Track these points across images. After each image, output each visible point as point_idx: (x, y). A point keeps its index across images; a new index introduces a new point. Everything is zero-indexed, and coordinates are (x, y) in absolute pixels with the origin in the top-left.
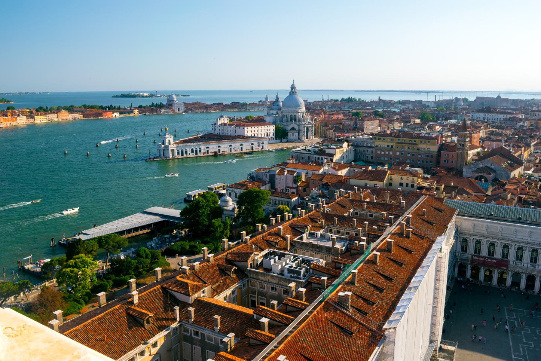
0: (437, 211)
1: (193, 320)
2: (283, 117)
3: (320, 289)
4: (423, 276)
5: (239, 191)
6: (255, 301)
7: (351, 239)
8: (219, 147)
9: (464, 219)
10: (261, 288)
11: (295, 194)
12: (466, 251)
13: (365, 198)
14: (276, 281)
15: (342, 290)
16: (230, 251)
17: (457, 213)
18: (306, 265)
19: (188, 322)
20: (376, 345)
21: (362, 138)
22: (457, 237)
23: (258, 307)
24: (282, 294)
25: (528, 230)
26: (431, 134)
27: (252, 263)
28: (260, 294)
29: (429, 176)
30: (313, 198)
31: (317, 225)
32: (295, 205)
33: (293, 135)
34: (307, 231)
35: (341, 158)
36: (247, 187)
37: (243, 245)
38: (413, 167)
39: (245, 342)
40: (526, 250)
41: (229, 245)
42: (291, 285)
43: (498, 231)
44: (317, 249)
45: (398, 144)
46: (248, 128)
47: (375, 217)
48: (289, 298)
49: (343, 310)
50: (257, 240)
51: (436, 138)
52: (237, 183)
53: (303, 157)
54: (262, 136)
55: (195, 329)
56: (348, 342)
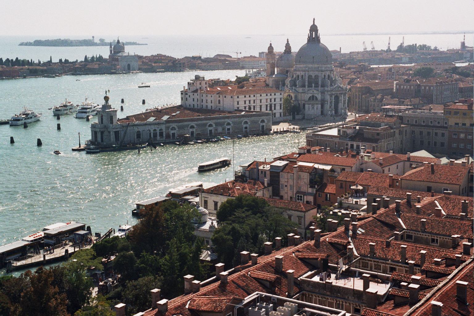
2: (297, 78)
11: (312, 204)
33: (313, 108)
44: (339, 295)
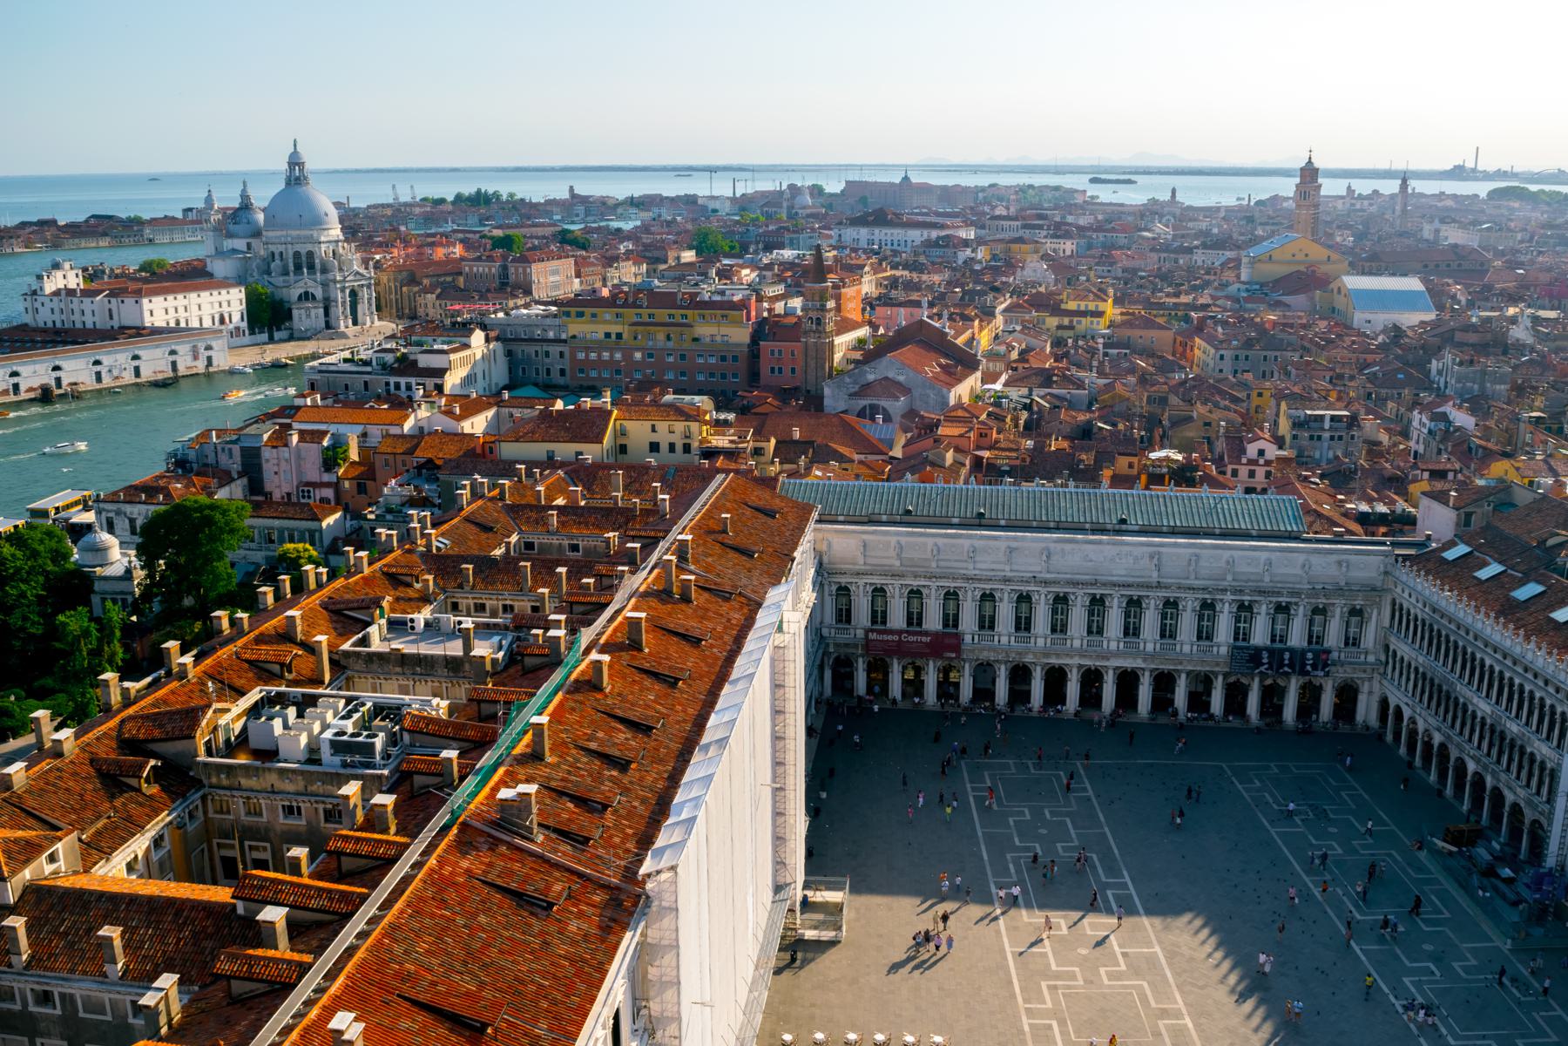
0: (761, 516)
1: (25, 957)
3: (440, 789)
4: (738, 707)
5: (141, 512)
6: (235, 859)
7: (521, 625)
8: (57, 368)
9: (837, 531)
10: (249, 813)
11: (333, 503)
12: (849, 621)
13: (550, 498)
14: (300, 784)
15: (510, 780)
16: (131, 711)
17: (815, 515)
18: (387, 722)
19: (10, 965)
20: (625, 928)
21: (529, 316)
22: (822, 585)
23: (245, 877)
24: (319, 823)
25: (1003, 545)
26: (727, 292)
27: (210, 740)
28: (250, 833)
29: (731, 417)
30: (389, 511)
31: (411, 593)
32: (335, 539)
33: (308, 316)
34: (382, 616)
35: (469, 380)
36: (168, 495)
37: (174, 684)
38: (684, 392)
39: (217, 993)
40: (1001, 600)
41: (125, 691)
42: (345, 791)
43: (929, 555)
45: (634, 328)
46: (154, 299)
47: (587, 551)
48: (344, 832)
49: (518, 841)
50: (219, 664)
51: (743, 305)
52: (131, 486)
53: (346, 386)
54: (205, 325)
55: (37, 987)
56: (542, 933)
